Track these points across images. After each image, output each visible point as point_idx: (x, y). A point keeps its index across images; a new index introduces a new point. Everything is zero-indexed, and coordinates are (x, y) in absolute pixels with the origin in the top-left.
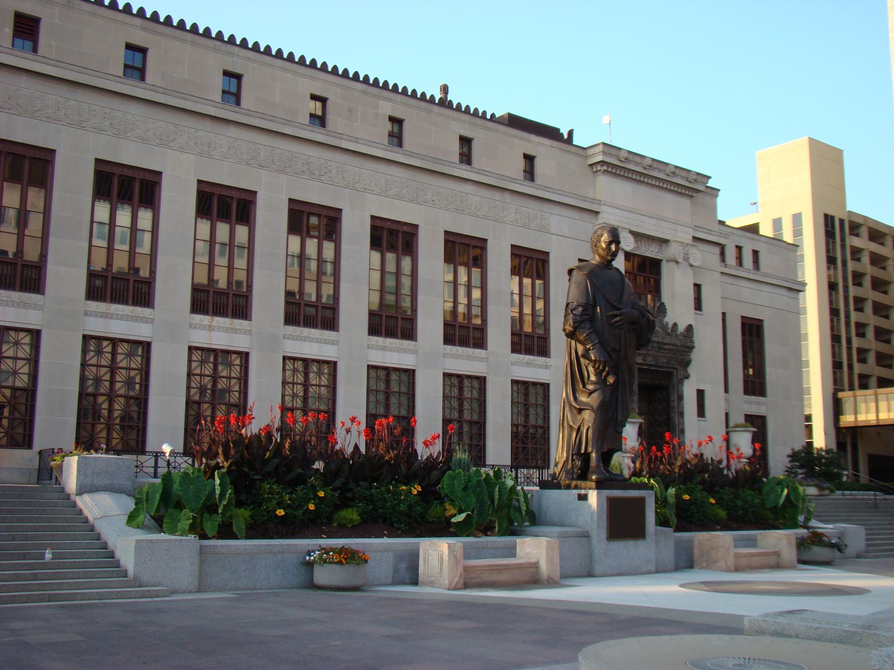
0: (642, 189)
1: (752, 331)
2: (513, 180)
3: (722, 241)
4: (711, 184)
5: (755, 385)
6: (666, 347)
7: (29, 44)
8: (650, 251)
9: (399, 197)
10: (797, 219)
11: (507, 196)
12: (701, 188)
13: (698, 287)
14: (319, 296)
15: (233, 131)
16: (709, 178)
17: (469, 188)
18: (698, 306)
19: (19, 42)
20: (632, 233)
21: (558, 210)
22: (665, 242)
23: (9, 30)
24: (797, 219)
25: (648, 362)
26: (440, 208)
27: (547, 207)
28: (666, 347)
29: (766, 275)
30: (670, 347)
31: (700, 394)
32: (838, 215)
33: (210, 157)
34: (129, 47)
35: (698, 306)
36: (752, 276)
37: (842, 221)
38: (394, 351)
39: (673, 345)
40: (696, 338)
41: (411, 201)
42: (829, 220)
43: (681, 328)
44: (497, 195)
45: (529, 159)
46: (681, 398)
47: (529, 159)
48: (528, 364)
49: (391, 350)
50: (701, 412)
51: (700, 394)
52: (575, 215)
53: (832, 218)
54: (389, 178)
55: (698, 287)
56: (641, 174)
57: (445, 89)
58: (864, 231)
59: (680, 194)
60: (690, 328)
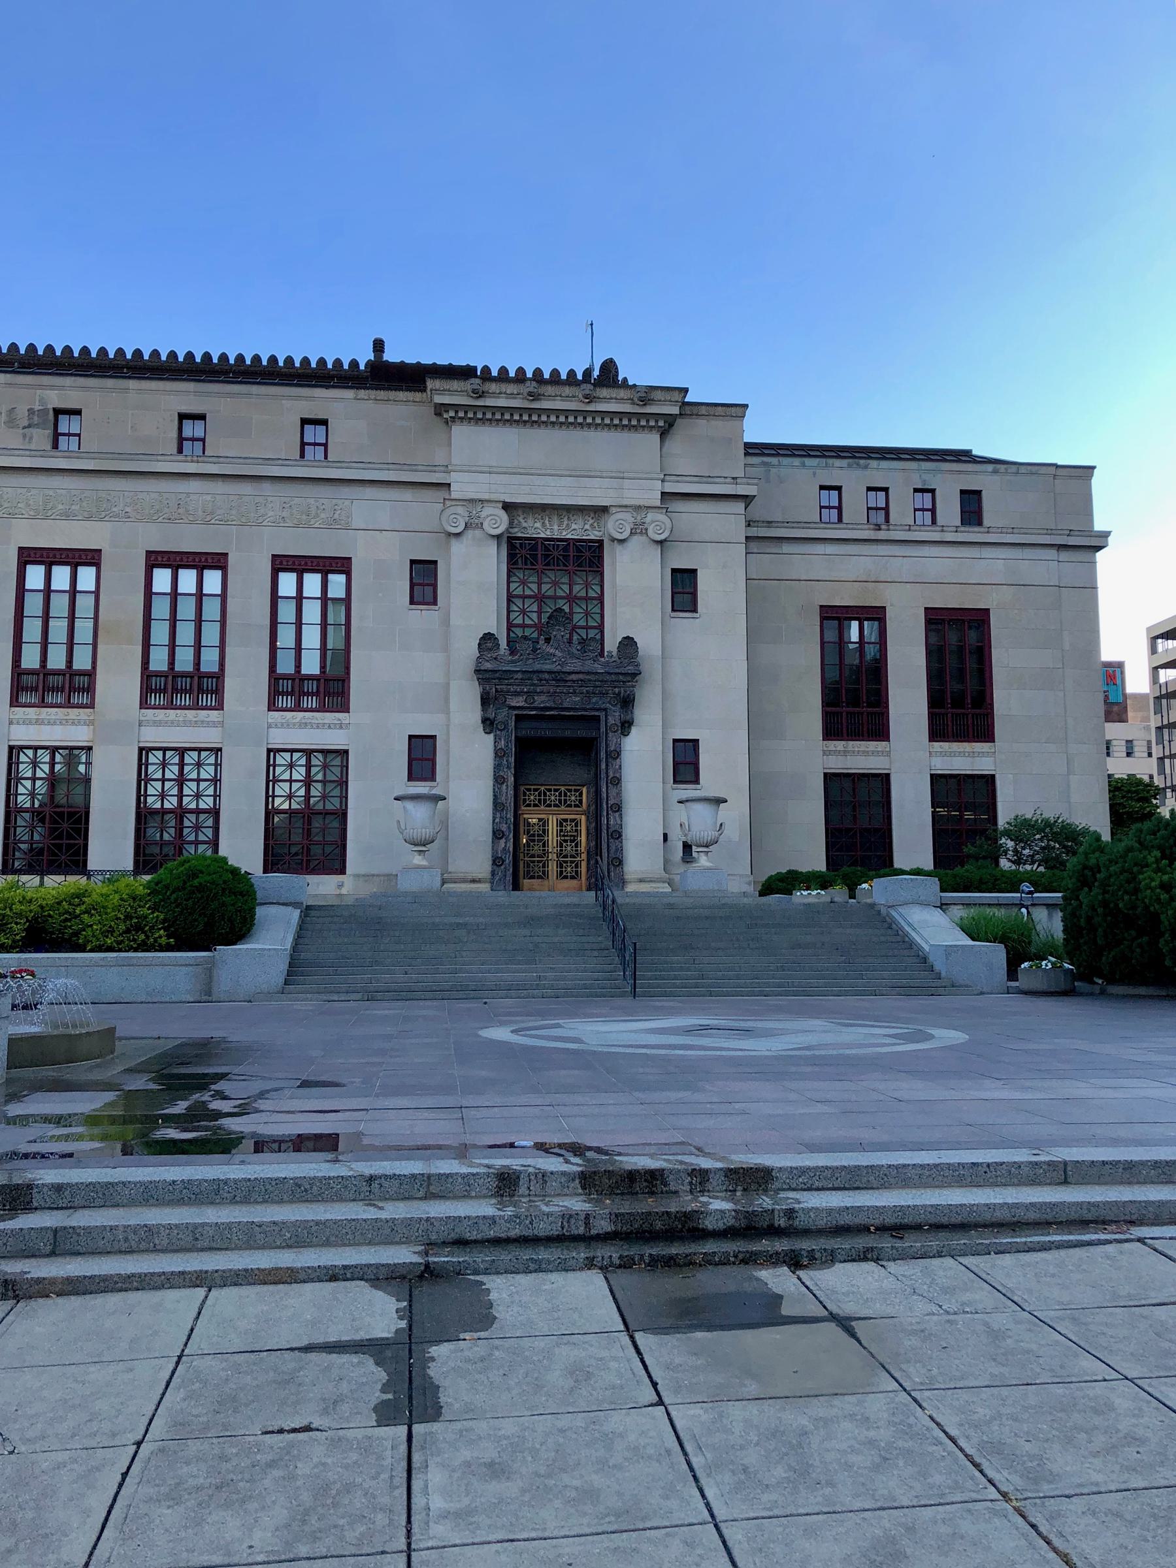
3: (741, 490)
6: (574, 677)
8: (577, 529)
9: (67, 516)
11: (267, 486)
12: (675, 410)
14: (197, 663)
17: (194, 485)
20: (507, 507)
21: (369, 492)
22: (604, 510)
25: (536, 704)
26: (140, 520)
27: (346, 491)
28: (574, 677)
30: (581, 676)
38: (55, 724)
39: (588, 673)
41: (88, 519)
44: (246, 488)
48: (303, 725)
49: (49, 723)
52: (408, 494)
54: (51, 493)
56: (530, 411)
59: (630, 427)
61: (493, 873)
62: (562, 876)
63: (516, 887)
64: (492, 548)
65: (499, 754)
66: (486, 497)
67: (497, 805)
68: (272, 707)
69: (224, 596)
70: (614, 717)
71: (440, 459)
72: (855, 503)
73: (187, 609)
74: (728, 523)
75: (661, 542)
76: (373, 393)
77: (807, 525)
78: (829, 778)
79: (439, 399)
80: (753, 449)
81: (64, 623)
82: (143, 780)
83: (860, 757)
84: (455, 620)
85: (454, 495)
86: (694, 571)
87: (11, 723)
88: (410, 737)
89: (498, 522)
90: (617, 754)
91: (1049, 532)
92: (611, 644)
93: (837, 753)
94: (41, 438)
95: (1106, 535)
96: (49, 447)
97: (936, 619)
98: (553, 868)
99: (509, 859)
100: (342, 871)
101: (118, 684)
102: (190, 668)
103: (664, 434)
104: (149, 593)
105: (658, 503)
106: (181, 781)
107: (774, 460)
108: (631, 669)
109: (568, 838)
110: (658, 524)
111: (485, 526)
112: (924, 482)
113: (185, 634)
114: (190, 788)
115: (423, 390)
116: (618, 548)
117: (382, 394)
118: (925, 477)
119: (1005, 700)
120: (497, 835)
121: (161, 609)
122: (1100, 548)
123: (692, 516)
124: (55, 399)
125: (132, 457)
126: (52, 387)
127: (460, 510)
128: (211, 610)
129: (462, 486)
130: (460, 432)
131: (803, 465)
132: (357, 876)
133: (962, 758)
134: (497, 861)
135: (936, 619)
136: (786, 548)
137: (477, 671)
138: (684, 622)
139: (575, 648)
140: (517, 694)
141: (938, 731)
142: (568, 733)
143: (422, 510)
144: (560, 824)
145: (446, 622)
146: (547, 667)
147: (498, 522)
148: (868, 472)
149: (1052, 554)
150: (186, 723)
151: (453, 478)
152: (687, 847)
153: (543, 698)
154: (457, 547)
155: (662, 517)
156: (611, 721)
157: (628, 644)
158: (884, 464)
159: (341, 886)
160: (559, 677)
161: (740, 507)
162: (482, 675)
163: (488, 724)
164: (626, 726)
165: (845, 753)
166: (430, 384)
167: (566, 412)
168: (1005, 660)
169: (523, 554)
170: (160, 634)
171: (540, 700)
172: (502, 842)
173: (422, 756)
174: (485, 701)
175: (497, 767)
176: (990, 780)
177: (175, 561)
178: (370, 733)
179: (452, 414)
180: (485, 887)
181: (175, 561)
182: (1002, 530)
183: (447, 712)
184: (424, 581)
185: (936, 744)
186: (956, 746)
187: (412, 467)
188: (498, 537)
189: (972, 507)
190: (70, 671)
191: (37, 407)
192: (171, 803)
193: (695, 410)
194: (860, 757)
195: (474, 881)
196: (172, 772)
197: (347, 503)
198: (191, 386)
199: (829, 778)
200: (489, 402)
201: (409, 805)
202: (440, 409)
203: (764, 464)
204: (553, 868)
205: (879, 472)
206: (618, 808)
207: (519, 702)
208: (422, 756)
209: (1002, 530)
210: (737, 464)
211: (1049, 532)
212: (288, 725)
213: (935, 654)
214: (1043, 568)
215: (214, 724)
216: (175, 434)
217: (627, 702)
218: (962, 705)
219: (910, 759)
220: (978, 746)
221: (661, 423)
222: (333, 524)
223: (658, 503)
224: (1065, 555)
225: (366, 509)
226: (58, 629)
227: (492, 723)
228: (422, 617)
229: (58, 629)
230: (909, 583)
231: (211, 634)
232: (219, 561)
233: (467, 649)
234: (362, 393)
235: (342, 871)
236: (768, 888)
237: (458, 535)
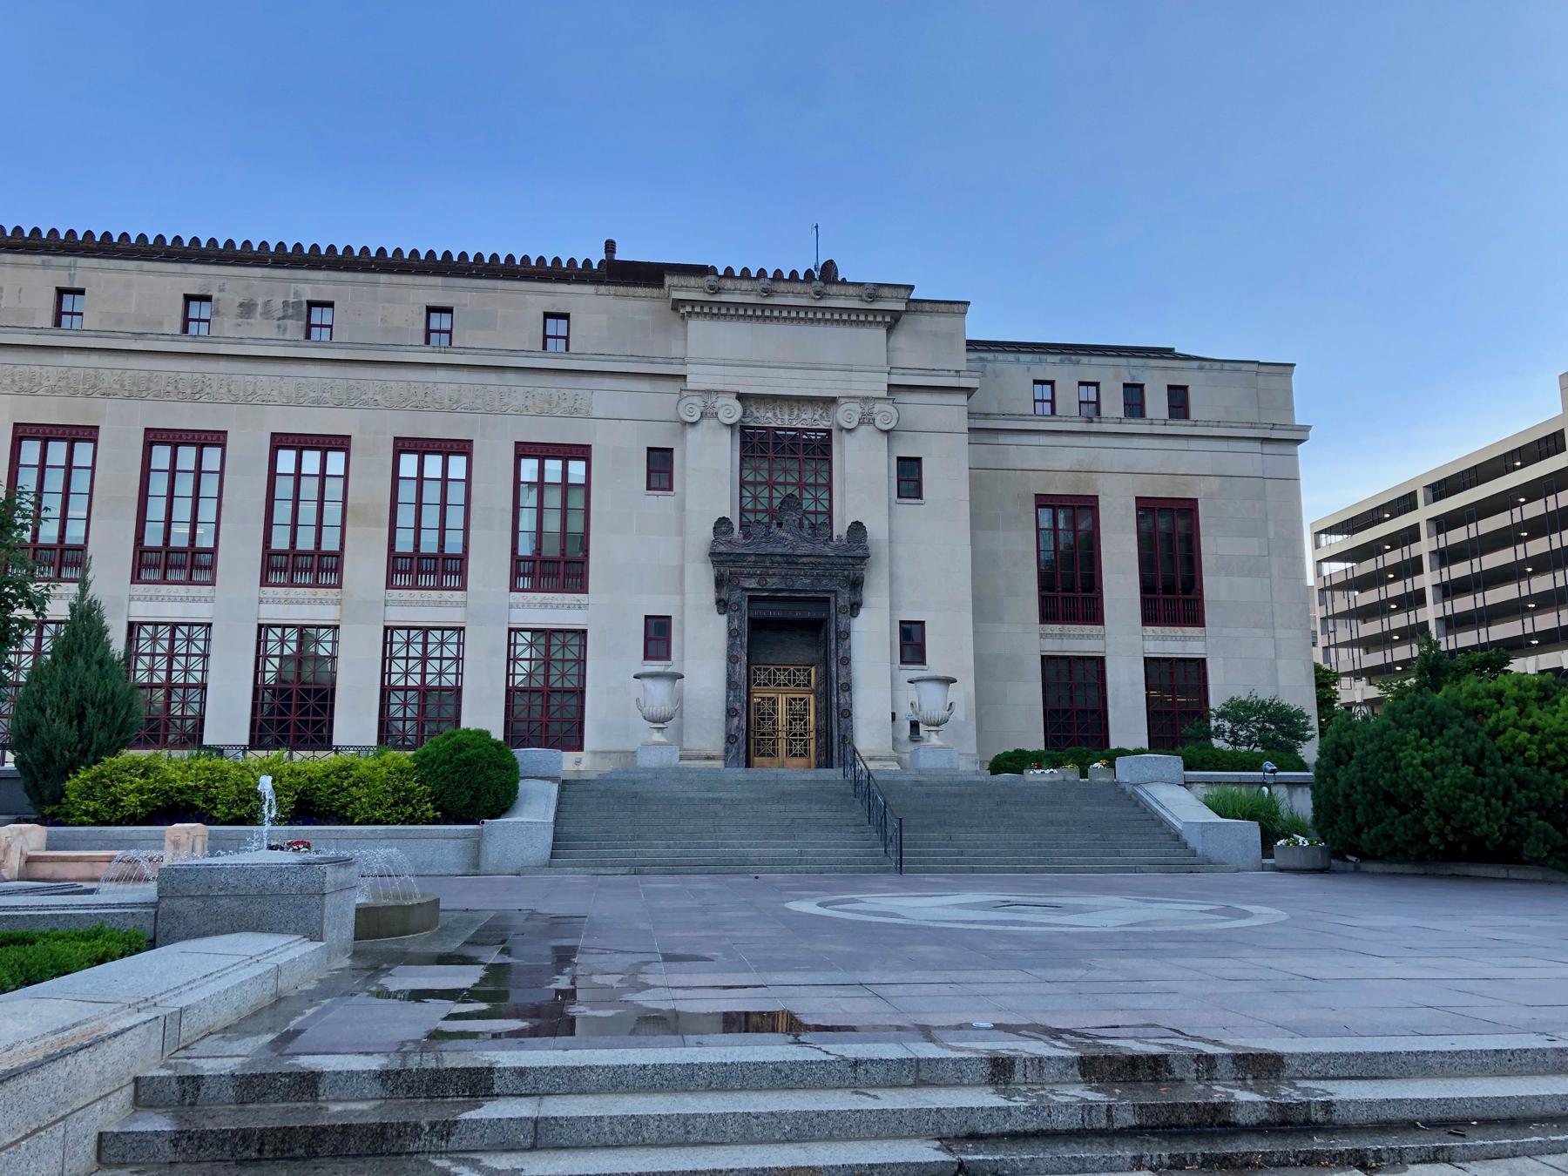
2: (528, 353)
3: (964, 383)
6: (804, 560)
8: (806, 419)
9: (318, 403)
11: (511, 378)
12: (901, 307)
15: (67, 359)
16: (912, 288)
17: (441, 375)
20: (741, 397)
21: (609, 383)
22: (831, 401)
26: (388, 408)
28: (804, 560)
33: (33, 394)
39: (818, 556)
41: (337, 406)
44: (491, 378)
48: (544, 606)
52: (644, 385)
56: (763, 306)
57: (610, 246)
59: (858, 323)
61: (727, 751)
62: (791, 753)
63: (748, 765)
64: (727, 433)
65: (732, 634)
66: (720, 387)
67: (731, 684)
68: (513, 588)
69: (468, 481)
70: (844, 598)
71: (677, 352)
72: (1068, 395)
73: (432, 493)
74: (953, 412)
75: (887, 432)
76: (612, 289)
77: (1022, 417)
78: (1046, 660)
79: (676, 295)
80: (973, 345)
81: (314, 506)
82: (387, 658)
83: (1075, 640)
84: (691, 505)
85: (690, 386)
86: (919, 460)
87: (261, 602)
88: (647, 617)
89: (734, 412)
90: (845, 635)
91: (1253, 426)
92: (840, 528)
93: (1052, 636)
94: (295, 328)
95: (1306, 429)
96: (302, 337)
97: (1145, 507)
98: (782, 746)
99: (742, 737)
100: (580, 748)
101: (365, 564)
102: (435, 550)
103: (890, 329)
104: (396, 478)
105: (885, 395)
106: (424, 659)
107: (989, 356)
108: (859, 552)
109: (798, 717)
110: (885, 414)
111: (720, 415)
112: (1133, 378)
113: (431, 517)
114: (433, 667)
115: (661, 285)
116: (847, 437)
117: (621, 290)
118: (1134, 372)
119: (1214, 586)
120: (731, 713)
121: (407, 492)
122: (1300, 441)
123: (918, 408)
124: (308, 293)
125: (382, 347)
126: (306, 281)
127: (697, 400)
128: (456, 494)
129: (698, 378)
130: (698, 328)
131: (1018, 360)
132: (594, 753)
133: (1174, 643)
134: (730, 738)
135: (1145, 507)
136: (1002, 439)
137: (712, 554)
138: (908, 509)
139: (806, 533)
140: (750, 576)
141: (1151, 616)
142: (798, 615)
143: (660, 399)
144: (790, 702)
145: (682, 508)
146: (779, 550)
147: (732, 411)
148: (1078, 368)
149: (1257, 446)
150: (429, 604)
151: (688, 370)
152: (914, 726)
153: (775, 580)
154: (692, 435)
155: (888, 407)
156: (841, 602)
157: (857, 528)
158: (1095, 360)
159: (578, 762)
160: (791, 560)
161: (962, 398)
162: (716, 557)
163: (722, 605)
164: (855, 608)
165: (1061, 636)
166: (668, 280)
167: (798, 308)
168: (1214, 547)
169: (756, 444)
170: (406, 516)
171: (773, 583)
172: (736, 720)
173: (658, 634)
174: (719, 582)
175: (731, 647)
176: (1201, 663)
177: (421, 447)
178: (606, 613)
179: (689, 309)
180: (719, 764)
181: (421, 447)
182: (1207, 424)
183: (682, 594)
184: (660, 467)
185: (1149, 628)
186: (1168, 630)
187: (650, 360)
188: (732, 426)
189: (1179, 400)
190: (318, 553)
191: (292, 299)
192: (413, 681)
193: (919, 306)
194: (1075, 640)
195: (708, 758)
196: (415, 651)
197: (588, 393)
198: (439, 280)
199: (1046, 660)
200: (724, 298)
201: (648, 683)
202: (677, 304)
203: (982, 359)
204: (782, 746)
205: (1091, 368)
206: (848, 687)
208: (658, 634)
209: (1207, 424)
210: (961, 358)
211: (1253, 426)
212: (529, 605)
213: (1147, 542)
214: (1247, 460)
215: (456, 605)
216: (423, 326)
217: (857, 585)
218: (1173, 591)
219: (1124, 643)
220: (1189, 631)
221: (888, 319)
222: (573, 413)
223: (885, 395)
224: (1268, 448)
225: (605, 398)
226: (308, 512)
227: (726, 605)
228: (660, 502)
229: (308, 512)
230: (1121, 475)
231: (455, 518)
232: (463, 448)
233: (703, 533)
234: (603, 289)
235: (580, 748)
236: (998, 766)
237: (694, 424)
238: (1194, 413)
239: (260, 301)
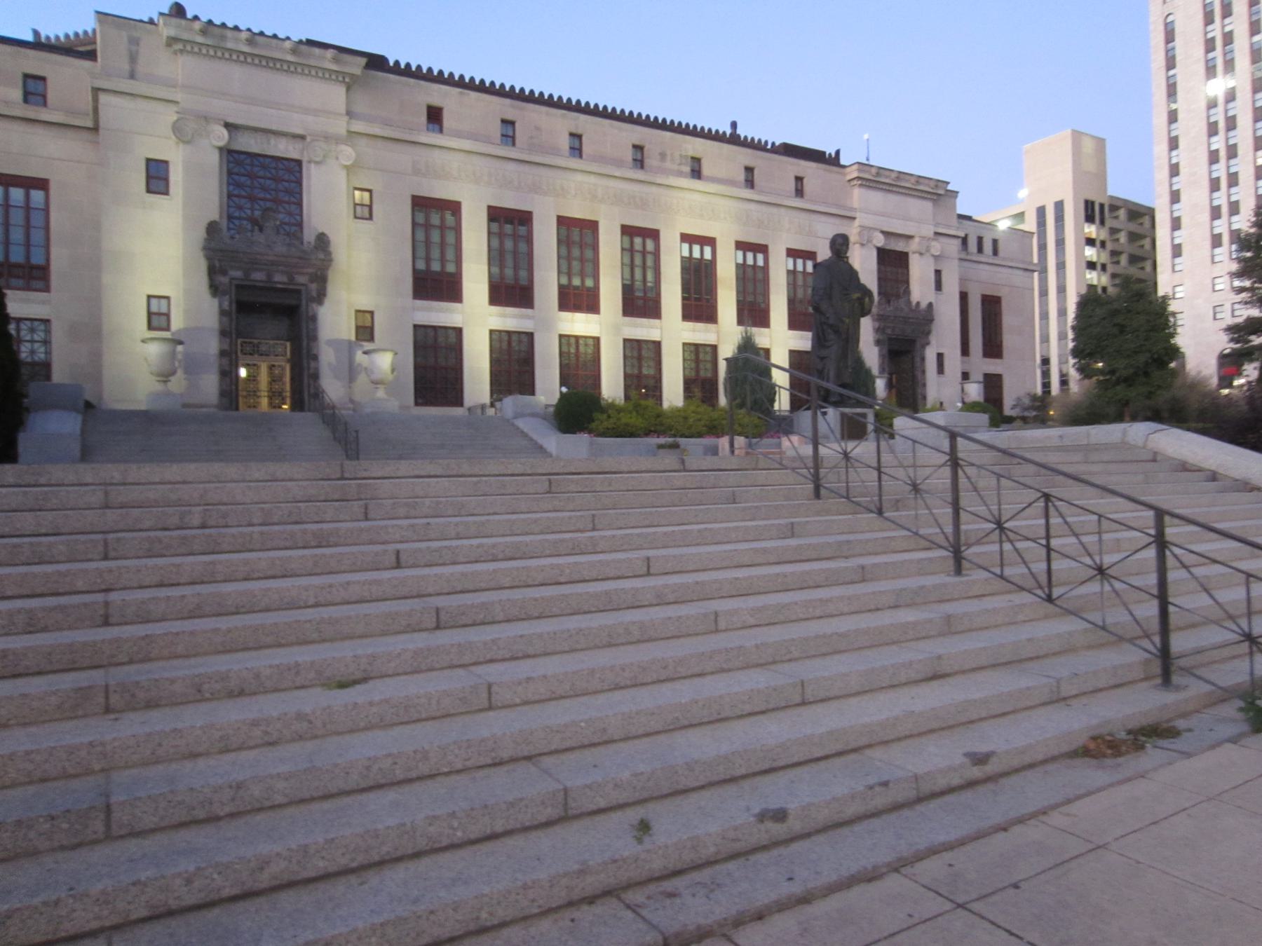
0: (891, 197)
1: (992, 305)
4: (950, 187)
5: (993, 348)
7: (437, 127)
8: (899, 246)
10: (1059, 206)
11: (782, 210)
12: (941, 192)
13: (938, 273)
16: (948, 183)
18: (939, 286)
19: (431, 126)
20: (883, 232)
21: (823, 218)
23: (424, 118)
24: (1059, 206)
27: (814, 216)
29: (1004, 259)
31: (940, 357)
32: (1098, 200)
34: (504, 121)
35: (939, 286)
36: (991, 261)
37: (1102, 206)
40: (935, 312)
42: (1089, 205)
43: (924, 305)
45: (799, 180)
46: (923, 359)
47: (799, 180)
50: (940, 369)
51: (940, 357)
53: (1093, 203)
55: (938, 273)
57: (734, 125)
58: (1122, 213)
60: (930, 305)
207: (889, 331)
210: (955, 220)
211: (1024, 262)
238: (1001, 253)
239: (669, 153)
